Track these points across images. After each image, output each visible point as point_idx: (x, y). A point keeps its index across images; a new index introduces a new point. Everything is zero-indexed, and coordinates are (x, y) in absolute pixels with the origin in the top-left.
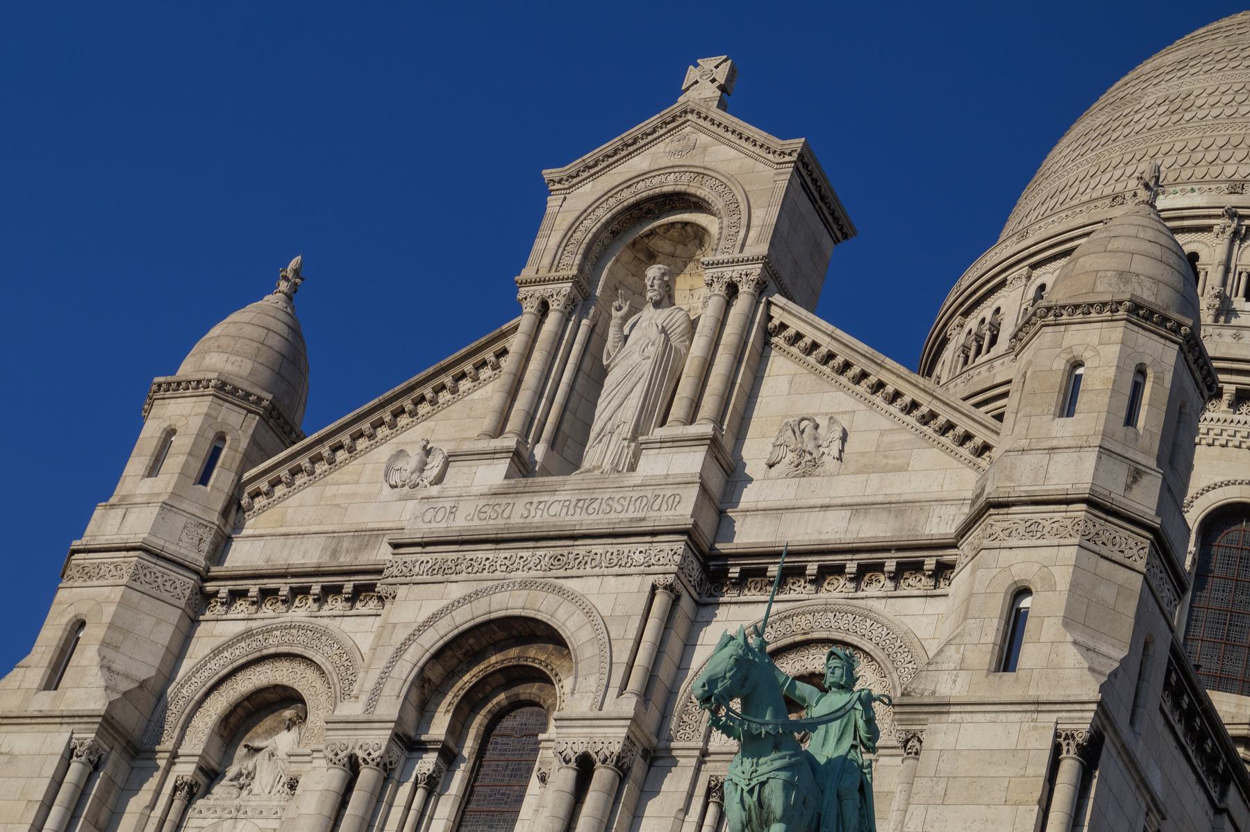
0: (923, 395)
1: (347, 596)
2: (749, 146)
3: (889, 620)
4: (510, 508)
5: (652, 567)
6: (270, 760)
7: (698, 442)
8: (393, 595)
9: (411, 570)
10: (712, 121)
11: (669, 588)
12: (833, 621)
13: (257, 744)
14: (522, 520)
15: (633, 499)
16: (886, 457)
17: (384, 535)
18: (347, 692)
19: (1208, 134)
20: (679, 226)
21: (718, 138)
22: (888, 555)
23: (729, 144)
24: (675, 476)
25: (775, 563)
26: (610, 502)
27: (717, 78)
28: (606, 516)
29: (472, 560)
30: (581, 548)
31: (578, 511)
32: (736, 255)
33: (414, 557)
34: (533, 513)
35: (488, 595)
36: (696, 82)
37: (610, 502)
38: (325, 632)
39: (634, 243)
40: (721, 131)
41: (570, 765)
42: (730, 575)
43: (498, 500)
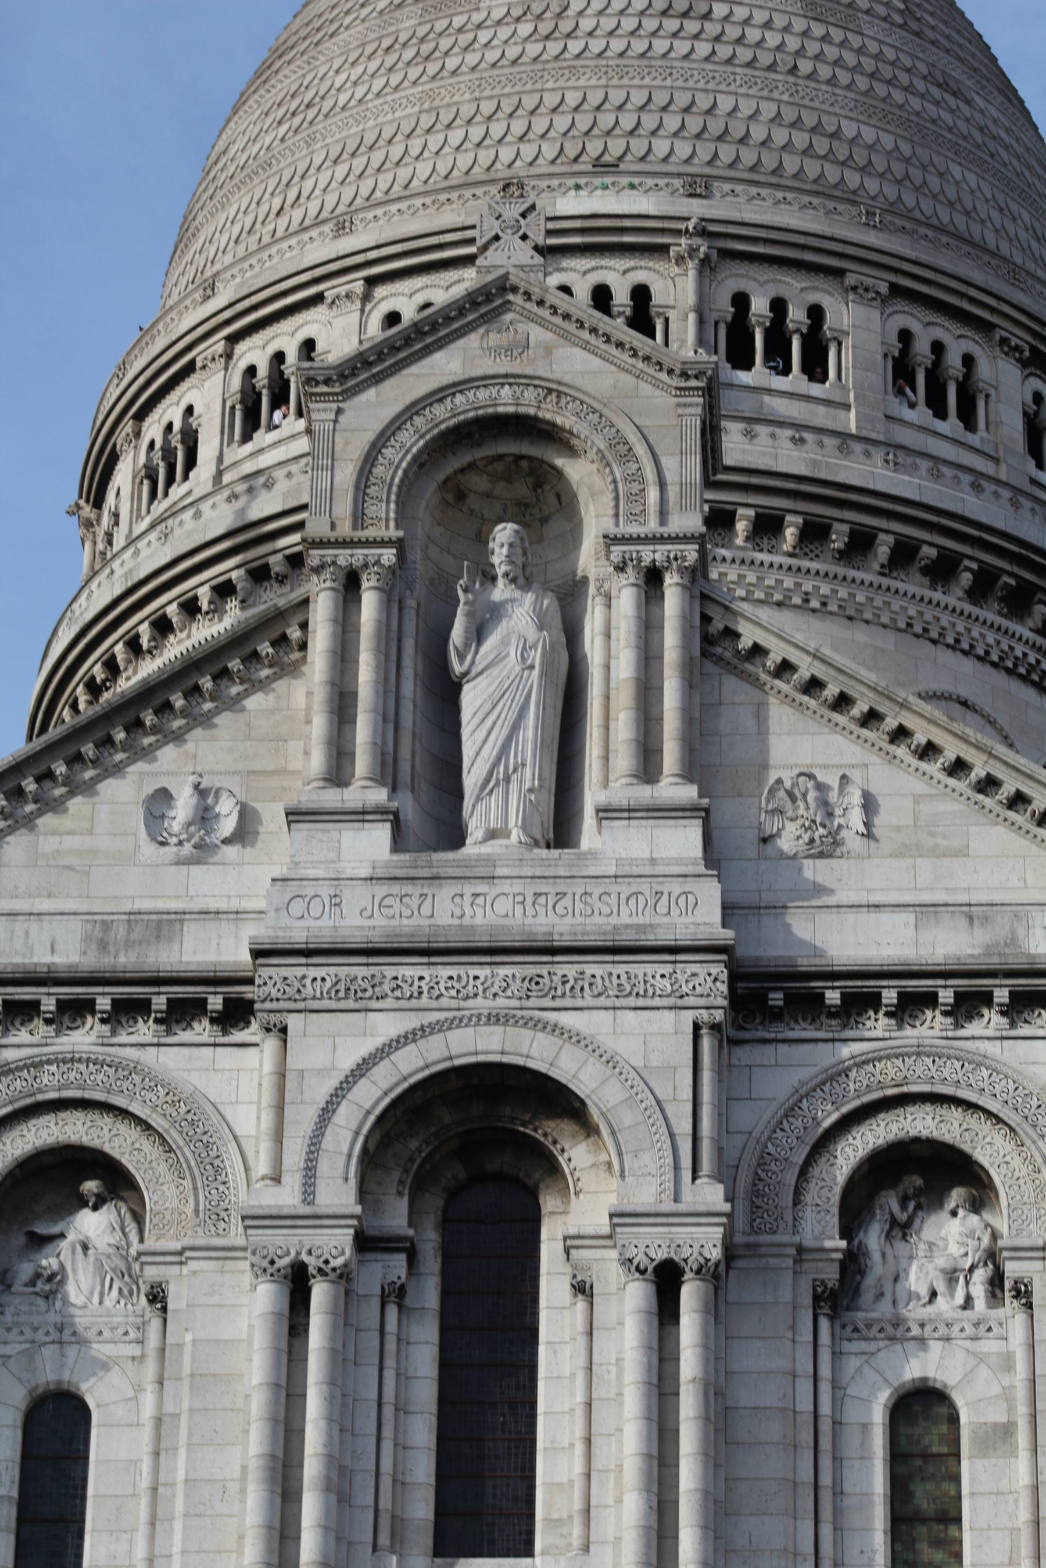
0: (972, 751)
1: (159, 1015)
2: (625, 357)
3: (1015, 1071)
4: (429, 901)
5: (686, 998)
6: (85, 1255)
7: (688, 814)
8: (279, 1026)
9: (299, 991)
10: (554, 310)
11: (715, 1027)
12: (933, 1069)
13: (42, 1229)
14: (456, 922)
15: (623, 897)
16: (932, 834)
17: (182, 921)
18: (207, 1160)
19: (615, 81)
20: (511, 459)
21: (565, 335)
22: (997, 982)
23: (586, 347)
24: (668, 861)
25: (833, 988)
26: (589, 899)
27: (529, 234)
28: (588, 920)
29: (396, 978)
30: (568, 968)
31: (541, 911)
32: (652, 525)
33: (299, 972)
34: (468, 911)
35: (439, 1031)
36: (497, 238)
37: (589, 899)
38: (135, 1068)
39: (447, 480)
40: (572, 327)
41: (647, 1276)
42: (770, 1003)
43: (407, 888)
